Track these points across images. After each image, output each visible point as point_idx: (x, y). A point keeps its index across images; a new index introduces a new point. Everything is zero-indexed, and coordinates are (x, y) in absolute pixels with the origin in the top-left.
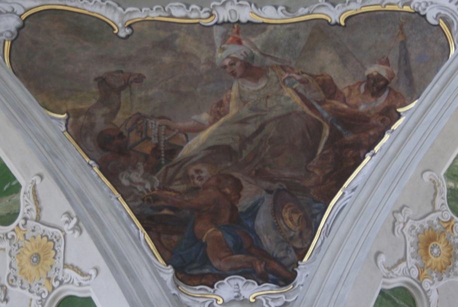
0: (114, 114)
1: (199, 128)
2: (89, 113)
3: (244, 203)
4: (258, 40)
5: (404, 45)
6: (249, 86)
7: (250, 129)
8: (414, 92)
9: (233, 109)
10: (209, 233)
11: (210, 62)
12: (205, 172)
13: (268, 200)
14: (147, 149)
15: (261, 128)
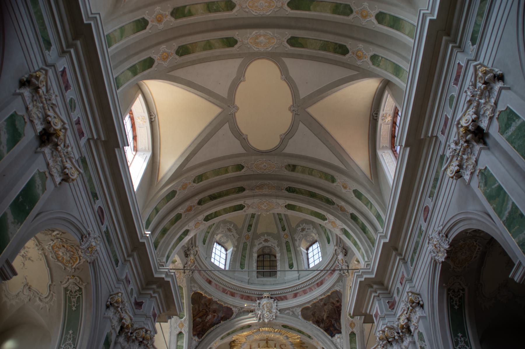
0: (315, 318)
1: (324, 315)
2: (313, 319)
3: (333, 323)
4: (324, 300)
5: (338, 295)
6: (326, 307)
7: (329, 312)
8: (341, 301)
9: (326, 311)
10: (332, 329)
11: (321, 305)
12: (328, 321)
13: (334, 321)
14: (321, 321)
15: (330, 312)
